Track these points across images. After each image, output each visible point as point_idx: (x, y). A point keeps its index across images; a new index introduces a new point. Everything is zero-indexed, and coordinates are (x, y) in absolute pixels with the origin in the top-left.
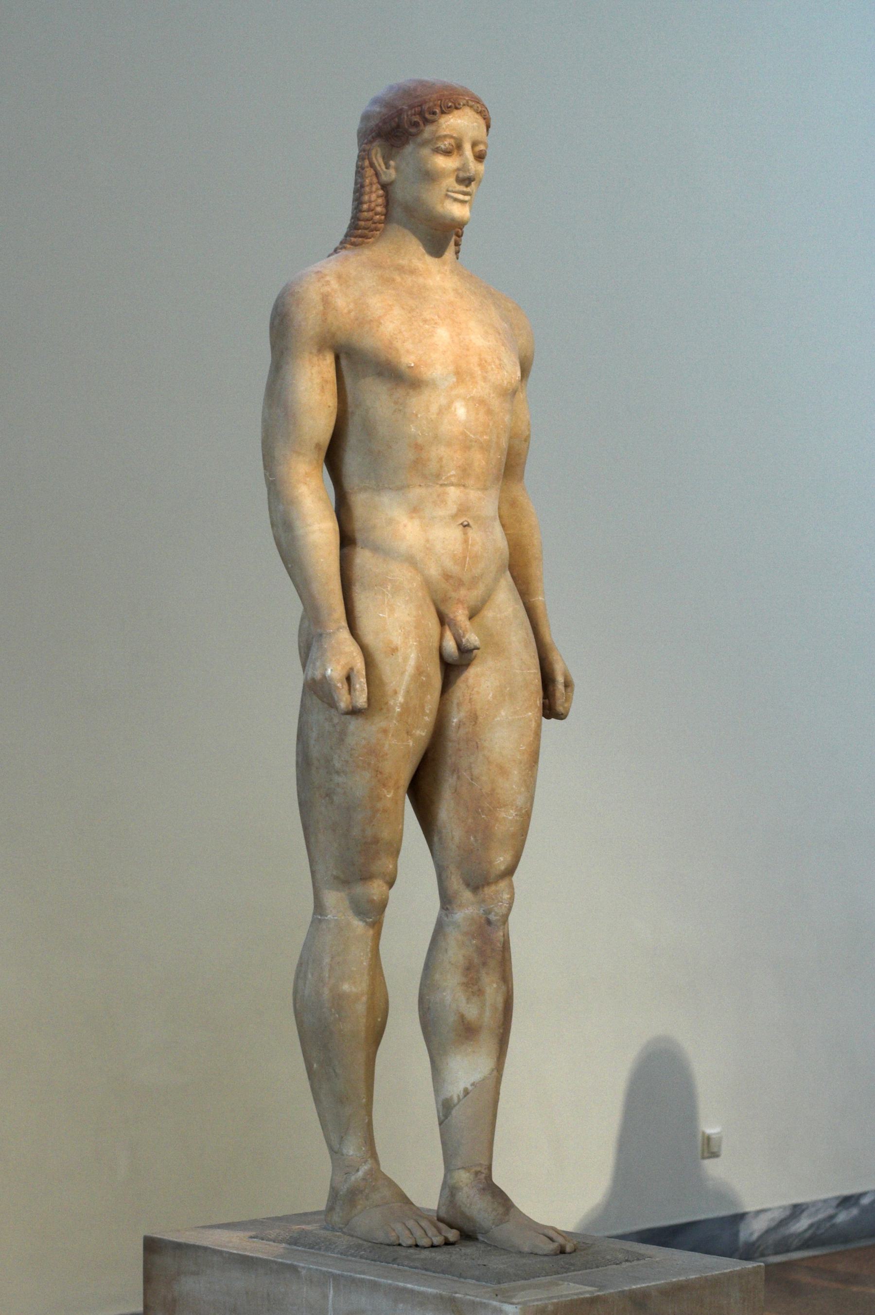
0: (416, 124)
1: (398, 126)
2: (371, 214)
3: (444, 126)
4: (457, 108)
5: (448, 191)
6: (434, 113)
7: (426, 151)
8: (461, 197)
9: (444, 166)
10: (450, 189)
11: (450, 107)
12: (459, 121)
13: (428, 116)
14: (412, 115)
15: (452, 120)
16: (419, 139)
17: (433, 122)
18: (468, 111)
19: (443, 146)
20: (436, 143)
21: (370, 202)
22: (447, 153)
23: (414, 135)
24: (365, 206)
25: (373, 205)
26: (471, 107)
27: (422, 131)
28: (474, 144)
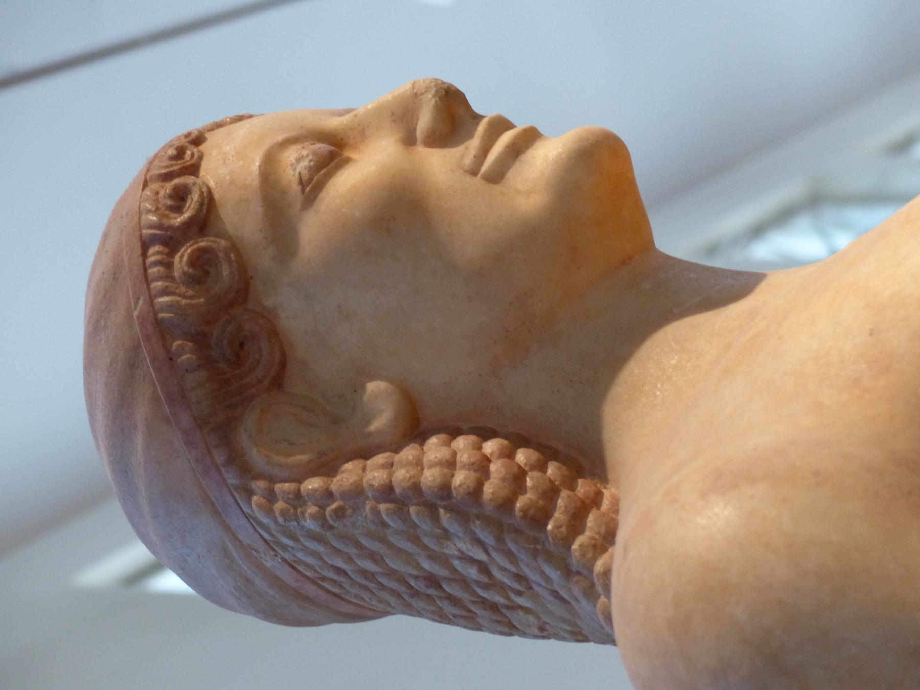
0: (203, 263)
1: (200, 340)
7: (313, 229)
9: (374, 167)
10: (468, 161)
14: (169, 277)
16: (263, 260)
17: (209, 202)
19: (305, 163)
20: (284, 193)
21: (451, 464)
23: (243, 290)
24: (460, 478)
25: (463, 457)
27: (234, 247)
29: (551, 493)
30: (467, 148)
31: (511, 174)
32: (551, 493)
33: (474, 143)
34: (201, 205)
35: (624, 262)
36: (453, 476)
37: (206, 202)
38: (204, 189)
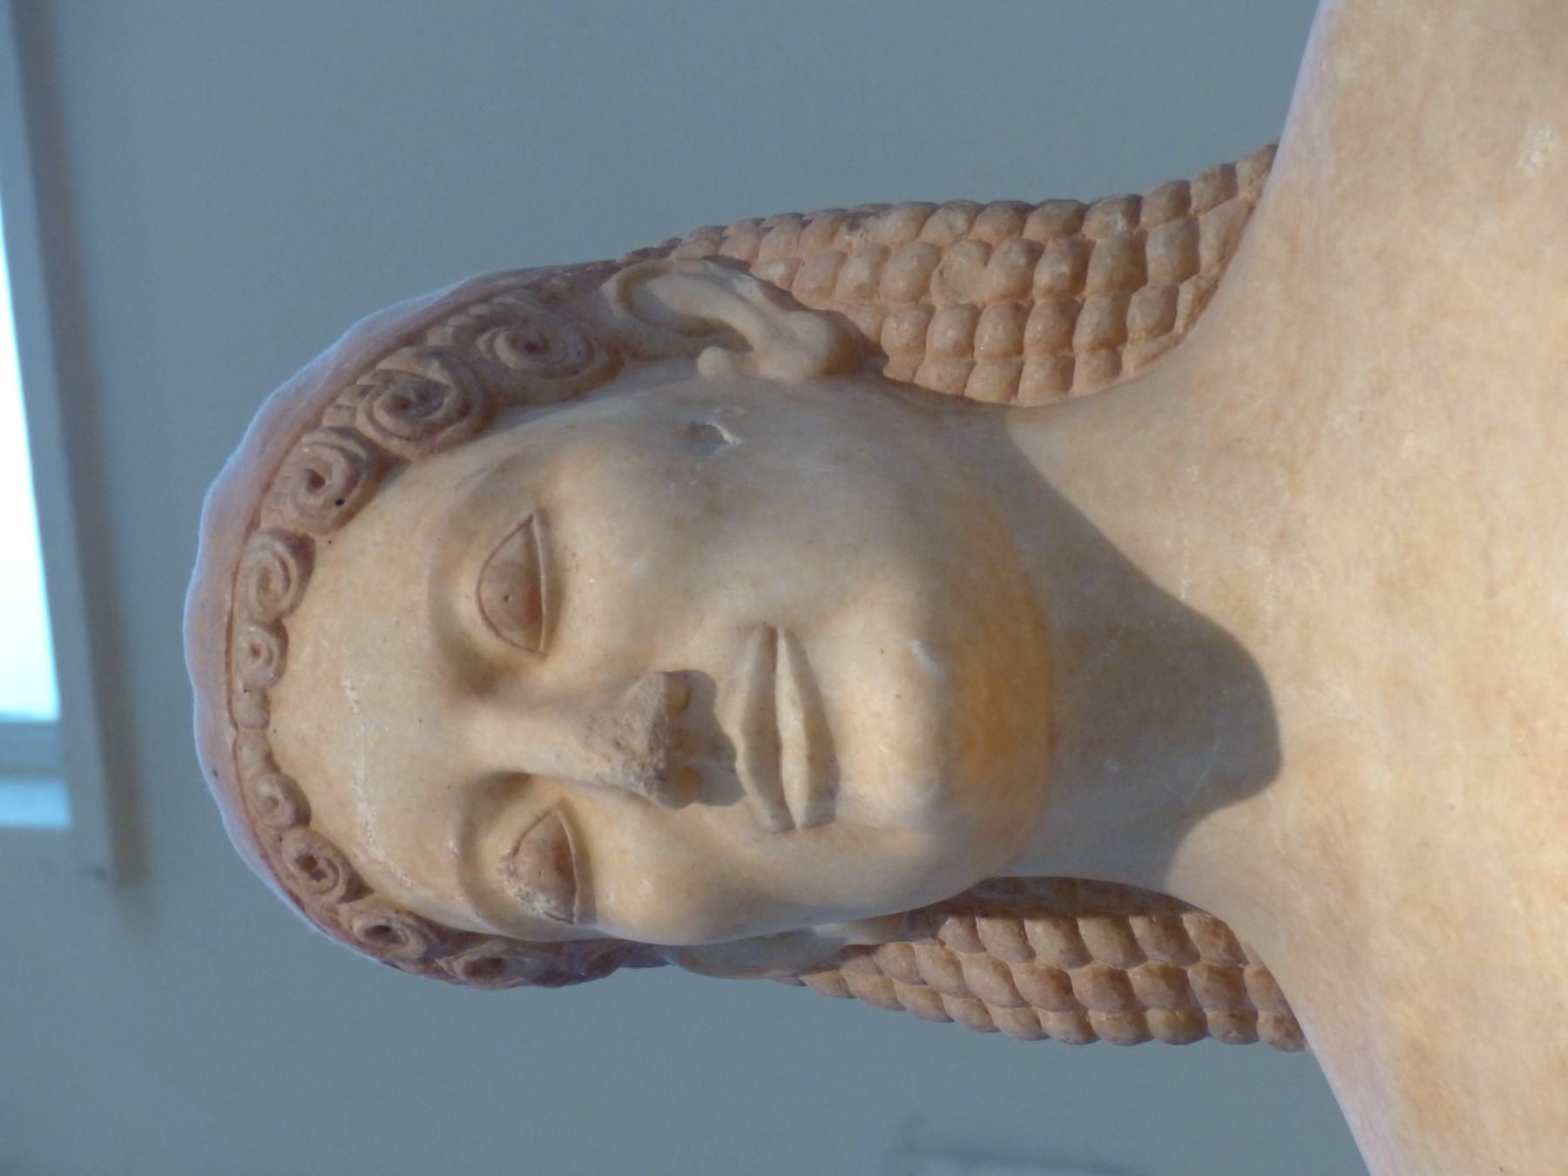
2: (1081, 980)
3: (427, 894)
4: (303, 816)
5: (788, 826)
6: (382, 933)
8: (794, 772)
9: (647, 887)
10: (767, 820)
11: (308, 863)
12: (365, 812)
13: (414, 946)
15: (380, 855)
18: (295, 726)
19: (541, 906)
22: (568, 864)
26: (265, 703)
28: (476, 679)
29: (1175, 979)
30: (748, 806)
31: (841, 811)
32: (1175, 979)
33: (753, 797)
34: (425, 937)
35: (1052, 741)
36: (1039, 1022)
37: (426, 930)
38: (410, 921)
